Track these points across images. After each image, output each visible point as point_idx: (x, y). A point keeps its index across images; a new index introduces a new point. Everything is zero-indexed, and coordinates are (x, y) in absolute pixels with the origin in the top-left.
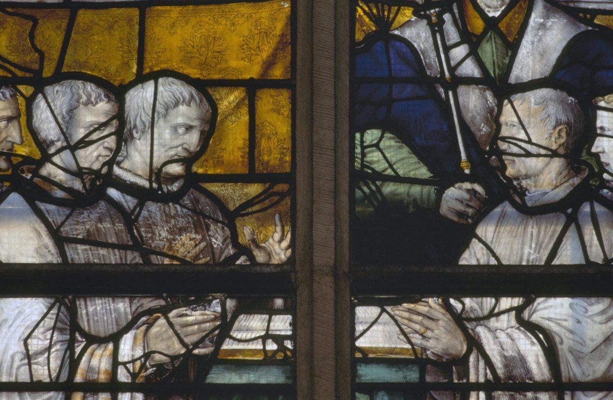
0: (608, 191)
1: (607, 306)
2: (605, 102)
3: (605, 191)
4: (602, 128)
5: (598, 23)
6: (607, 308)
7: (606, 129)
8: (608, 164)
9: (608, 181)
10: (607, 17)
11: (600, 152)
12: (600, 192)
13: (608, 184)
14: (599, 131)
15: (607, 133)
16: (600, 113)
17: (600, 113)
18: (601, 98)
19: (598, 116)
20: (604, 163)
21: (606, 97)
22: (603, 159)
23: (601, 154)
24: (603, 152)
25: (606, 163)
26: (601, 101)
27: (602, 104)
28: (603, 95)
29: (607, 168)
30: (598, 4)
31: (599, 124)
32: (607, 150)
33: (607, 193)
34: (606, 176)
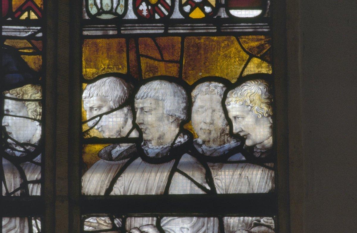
0: (10, 150)
1: (7, 222)
2: (10, 94)
3: (8, 150)
4: (8, 111)
5: (7, 44)
6: (6, 224)
7: (10, 111)
8: (10, 133)
9: (10, 144)
10: (13, 40)
11: (6, 126)
12: (5, 151)
13: (10, 146)
14: (5, 112)
15: (11, 113)
16: (7, 101)
17: (6, 100)
18: (7, 92)
19: (5, 103)
20: (8, 132)
21: (11, 91)
22: (8, 130)
23: (6, 127)
24: (8, 126)
25: (9, 132)
26: (7, 93)
27: (8, 95)
28: (9, 90)
29: (10, 135)
30: (7, 33)
31: (6, 107)
32: (10, 124)
33: (10, 151)
34: (9, 140)
